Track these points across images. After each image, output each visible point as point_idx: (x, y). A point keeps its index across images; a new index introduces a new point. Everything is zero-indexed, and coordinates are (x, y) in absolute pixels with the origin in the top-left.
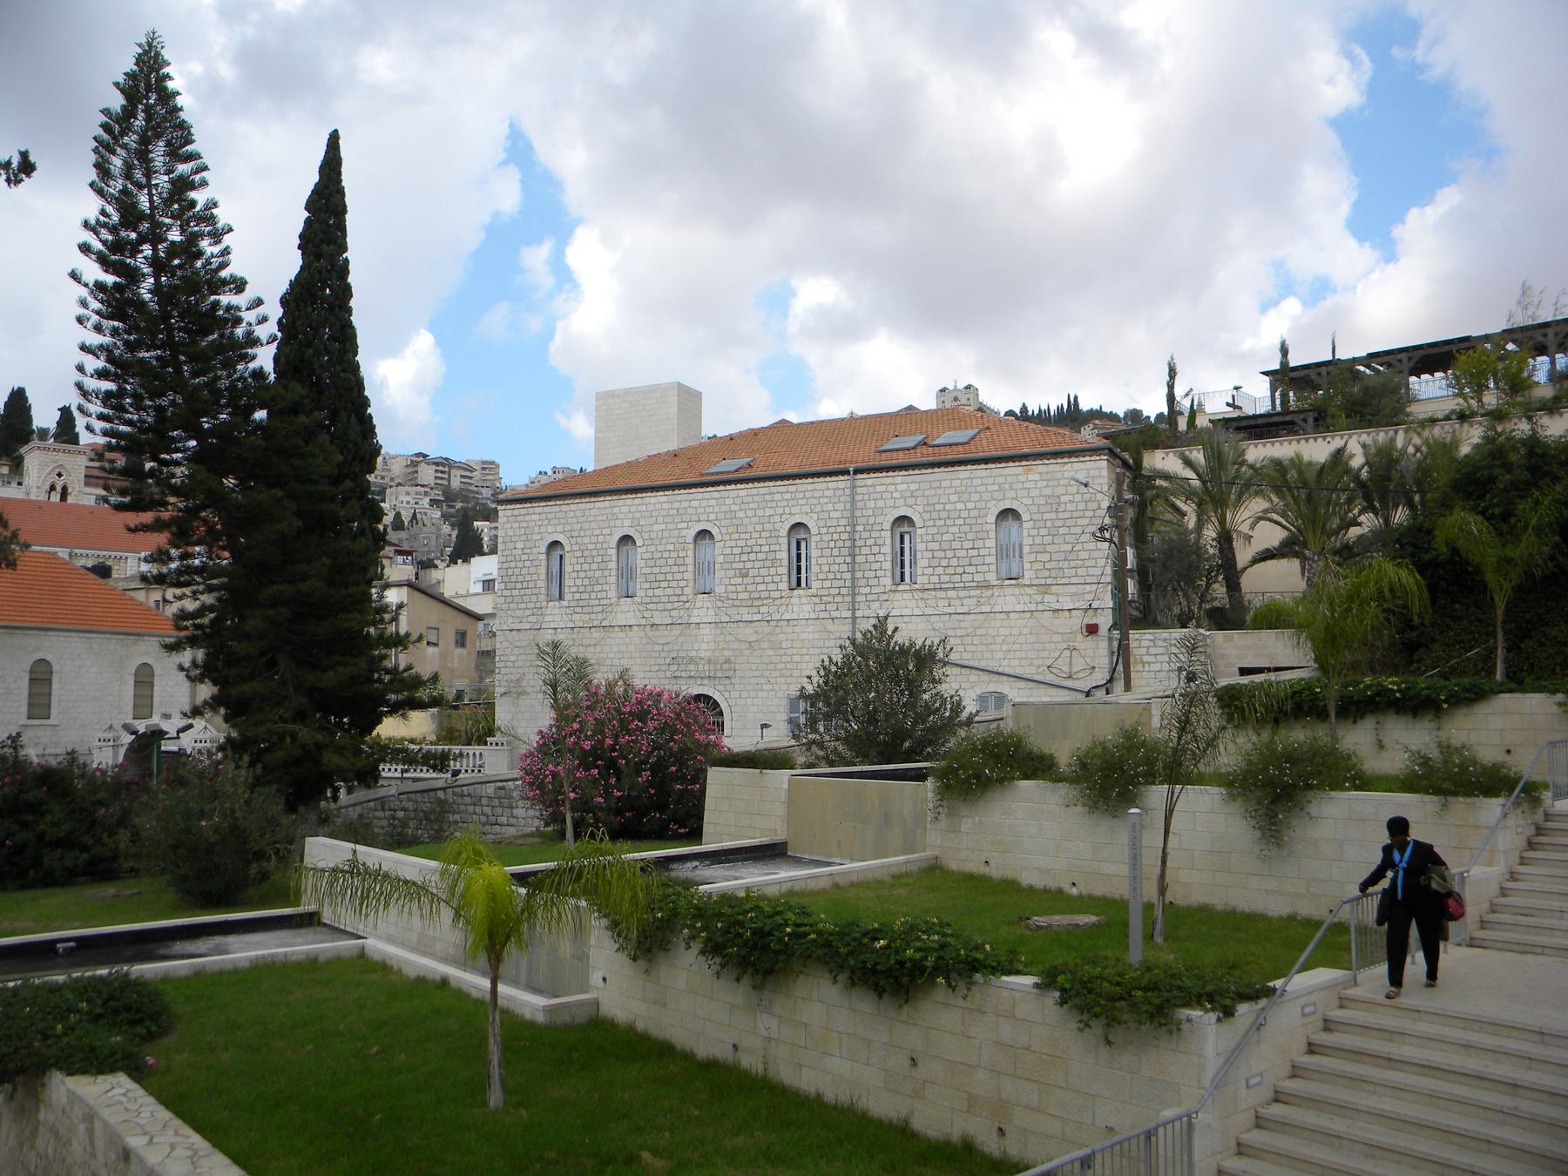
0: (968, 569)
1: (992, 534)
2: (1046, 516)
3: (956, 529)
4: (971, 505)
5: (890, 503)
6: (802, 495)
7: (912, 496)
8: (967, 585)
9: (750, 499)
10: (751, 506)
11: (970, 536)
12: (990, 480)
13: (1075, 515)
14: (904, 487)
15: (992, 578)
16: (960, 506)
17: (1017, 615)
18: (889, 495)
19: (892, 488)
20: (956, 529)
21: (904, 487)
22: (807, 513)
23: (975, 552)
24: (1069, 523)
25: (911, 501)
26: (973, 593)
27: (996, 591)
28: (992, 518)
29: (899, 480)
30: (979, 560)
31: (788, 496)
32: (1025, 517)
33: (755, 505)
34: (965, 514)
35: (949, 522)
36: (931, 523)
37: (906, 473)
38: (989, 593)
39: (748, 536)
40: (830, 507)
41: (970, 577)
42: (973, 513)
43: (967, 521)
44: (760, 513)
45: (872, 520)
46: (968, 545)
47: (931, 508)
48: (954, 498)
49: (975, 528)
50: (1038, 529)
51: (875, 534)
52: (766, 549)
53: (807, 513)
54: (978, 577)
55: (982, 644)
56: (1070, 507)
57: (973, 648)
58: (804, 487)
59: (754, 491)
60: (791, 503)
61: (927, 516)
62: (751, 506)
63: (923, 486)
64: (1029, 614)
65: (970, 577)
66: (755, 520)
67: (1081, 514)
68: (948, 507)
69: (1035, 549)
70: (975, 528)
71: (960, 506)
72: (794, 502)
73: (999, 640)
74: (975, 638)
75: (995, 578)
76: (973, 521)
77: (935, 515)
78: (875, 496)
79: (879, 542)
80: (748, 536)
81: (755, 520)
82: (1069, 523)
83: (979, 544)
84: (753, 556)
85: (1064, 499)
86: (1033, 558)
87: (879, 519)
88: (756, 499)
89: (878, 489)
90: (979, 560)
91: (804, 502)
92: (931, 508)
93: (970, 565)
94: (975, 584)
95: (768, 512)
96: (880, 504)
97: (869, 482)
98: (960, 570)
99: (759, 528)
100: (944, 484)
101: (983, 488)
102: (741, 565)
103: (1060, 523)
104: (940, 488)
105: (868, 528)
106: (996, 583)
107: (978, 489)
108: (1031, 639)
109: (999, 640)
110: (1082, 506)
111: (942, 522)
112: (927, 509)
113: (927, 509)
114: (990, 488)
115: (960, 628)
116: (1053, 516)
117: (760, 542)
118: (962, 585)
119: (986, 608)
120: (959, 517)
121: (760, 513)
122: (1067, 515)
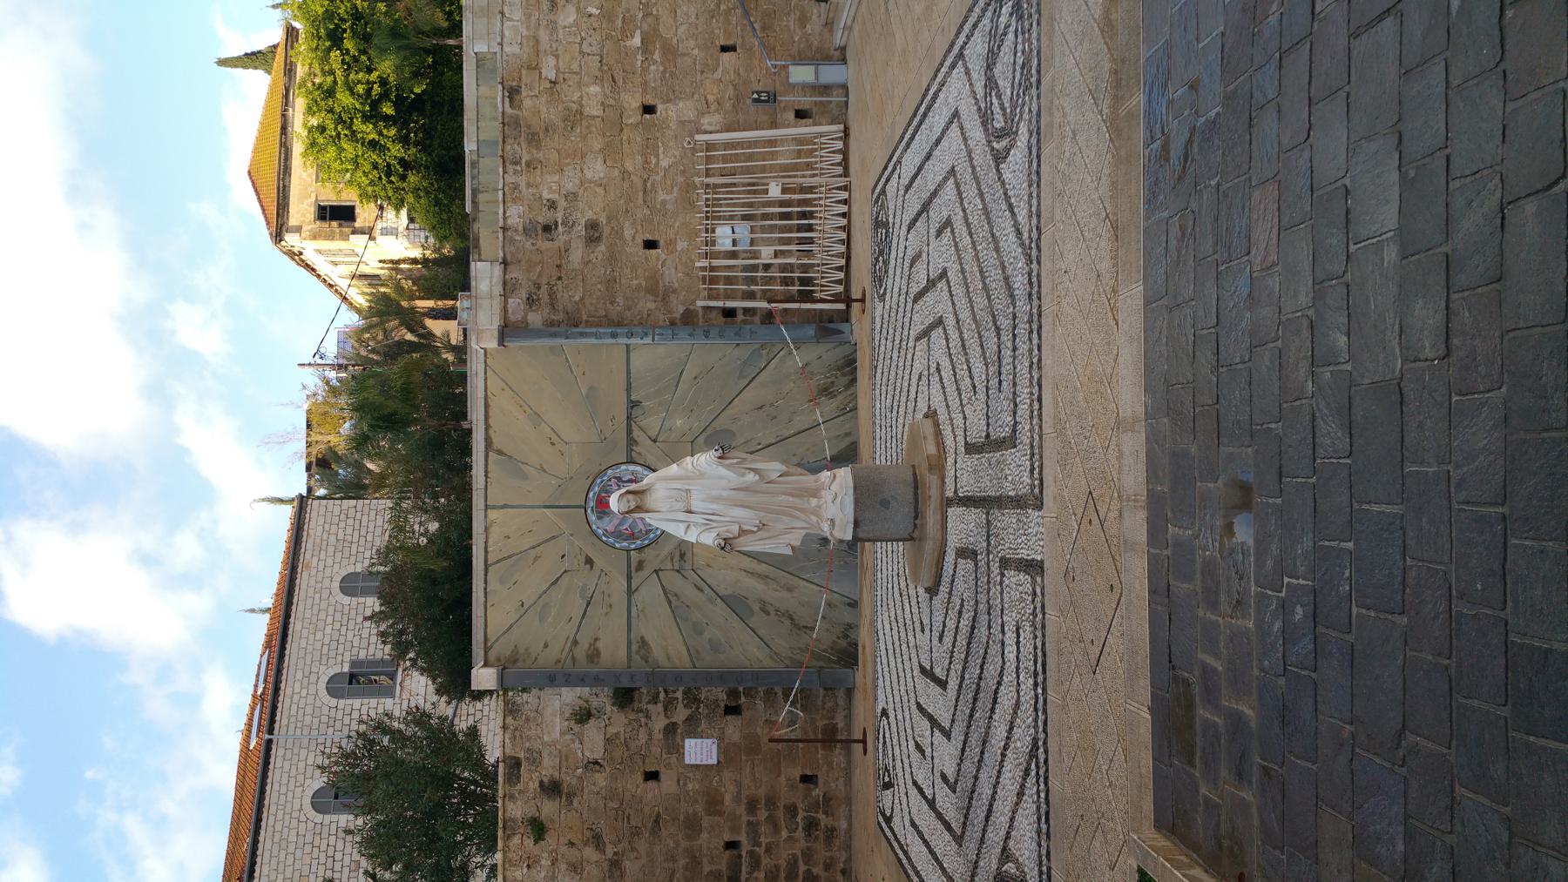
2: (354, 552)
3: (350, 634)
4: (330, 619)
5: (310, 699)
6: (283, 797)
7: (309, 677)
9: (274, 861)
10: (282, 858)
12: (309, 601)
13: (357, 527)
14: (297, 685)
16: (328, 630)
18: (303, 700)
19: (296, 697)
20: (350, 634)
21: (297, 685)
22: (303, 791)
24: (363, 532)
25: (313, 678)
29: (289, 691)
31: (280, 813)
33: (283, 853)
34: (337, 625)
35: (342, 640)
36: (339, 658)
37: (284, 682)
39: (315, 862)
40: (302, 765)
43: (344, 622)
44: (292, 848)
45: (325, 719)
47: (325, 658)
48: (319, 635)
51: (340, 716)
52: (333, 838)
53: (303, 791)
56: (349, 531)
58: (275, 794)
59: (267, 854)
60: (288, 810)
61: (332, 662)
62: (282, 858)
63: (301, 662)
66: (299, 854)
67: (357, 523)
68: (327, 641)
71: (328, 630)
72: (289, 806)
76: (345, 617)
77: (333, 654)
78: (300, 715)
79: (348, 711)
80: (315, 862)
81: (299, 854)
82: (363, 532)
84: (338, 856)
85: (341, 536)
87: (325, 710)
88: (275, 853)
89: (293, 712)
91: (290, 795)
92: (325, 658)
95: (293, 838)
96: (309, 710)
97: (285, 722)
99: (308, 848)
100: (303, 644)
101: (316, 608)
102: (346, 870)
103: (363, 539)
104: (306, 649)
105: (331, 723)
107: (315, 612)
110: (350, 522)
111: (341, 647)
112: (324, 662)
113: (324, 662)
114: (317, 601)
116: (354, 546)
117: (323, 848)
121: (292, 848)
122: (356, 533)
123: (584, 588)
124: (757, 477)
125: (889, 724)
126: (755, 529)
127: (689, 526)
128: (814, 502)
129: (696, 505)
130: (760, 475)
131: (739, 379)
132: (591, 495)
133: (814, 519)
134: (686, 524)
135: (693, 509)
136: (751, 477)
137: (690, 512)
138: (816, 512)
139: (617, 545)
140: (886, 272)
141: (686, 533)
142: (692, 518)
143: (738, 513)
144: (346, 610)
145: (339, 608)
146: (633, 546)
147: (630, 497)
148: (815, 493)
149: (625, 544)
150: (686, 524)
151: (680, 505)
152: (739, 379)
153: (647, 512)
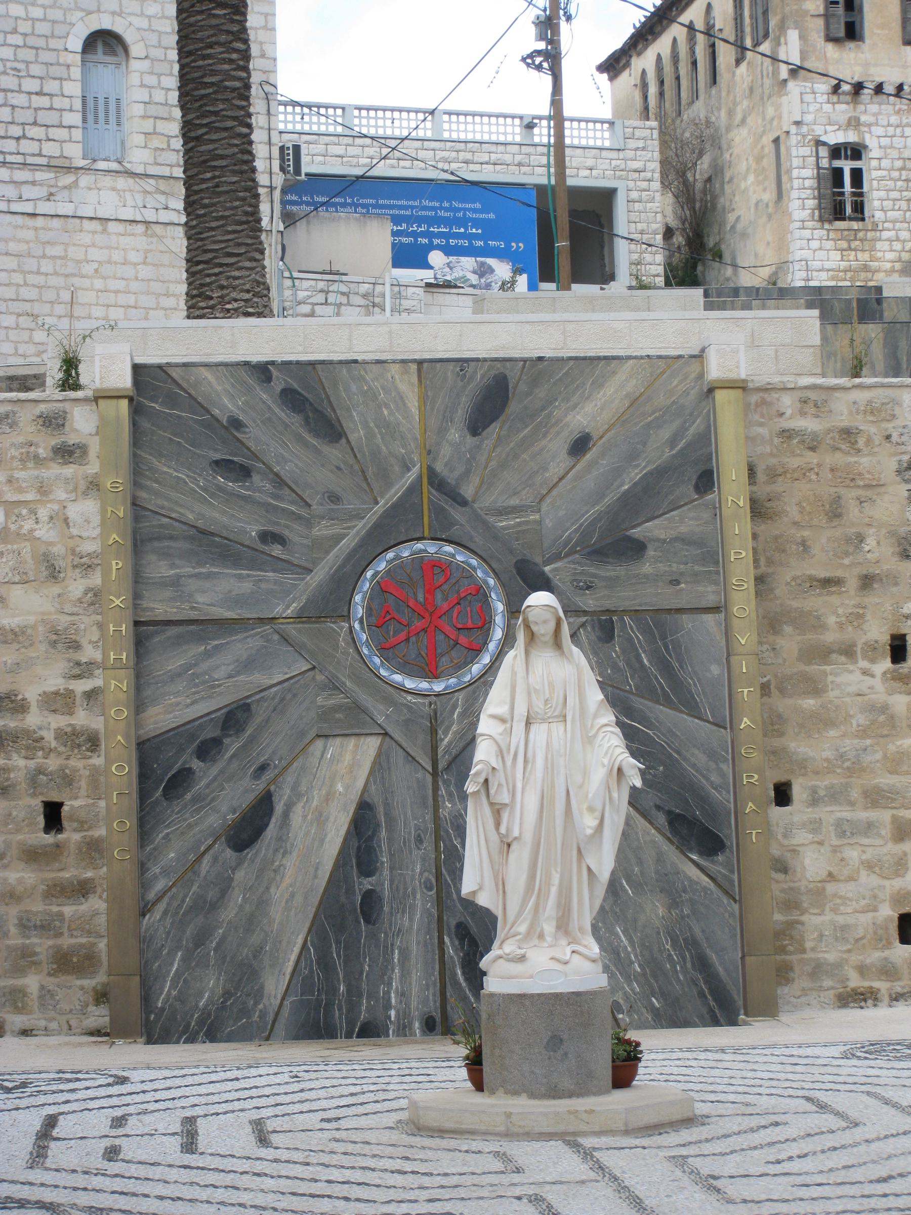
0: (33, 132)
1: (76, 72)
8: (30, 160)
11: (36, 70)
15: (74, 152)
17: (120, 227)
23: (44, 101)
26: (40, 176)
27: (85, 180)
28: (76, 44)
30: (50, 118)
32: (136, 50)
34: (25, 27)
38: (69, 179)
41: (32, 147)
42: (43, 28)
43: (31, 41)
46: (31, 85)
49: (45, 56)
50: (159, 75)
54: (50, 149)
55: (56, 273)
57: (40, 280)
64: (140, 228)
65: (32, 147)
69: (153, 110)
70: (45, 56)
73: (89, 269)
74: (44, 262)
75: (80, 154)
76: (41, 42)
83: (51, 86)
86: (148, 125)
90: (50, 118)
93: (35, 123)
94: (44, 161)
98: (16, 131)
106: (82, 163)
108: (145, 272)
109: (89, 269)
115: (15, 239)
118: (19, 159)
119: (66, 209)
120: (15, 31)
123: (278, 539)
124: (589, 832)
125: (109, 1085)
126: (503, 830)
127: (502, 720)
128: (549, 928)
129: (539, 732)
130: (593, 836)
131: (669, 813)
132: (449, 549)
133: (522, 928)
134: (508, 717)
135: (534, 728)
136: (589, 822)
137: (528, 724)
138: (535, 934)
139: (358, 598)
140: (899, 1059)
141: (493, 717)
142: (519, 727)
143: (530, 802)
144: (53, 43)
145: (60, 30)
146: (357, 626)
147: (552, 625)
148: (563, 925)
149: (360, 612)
150: (508, 717)
151: (539, 706)
152: (669, 813)
153: (527, 653)
